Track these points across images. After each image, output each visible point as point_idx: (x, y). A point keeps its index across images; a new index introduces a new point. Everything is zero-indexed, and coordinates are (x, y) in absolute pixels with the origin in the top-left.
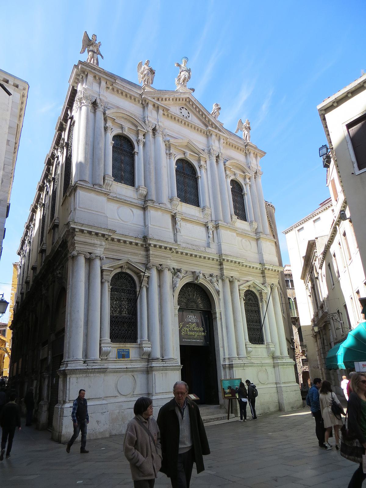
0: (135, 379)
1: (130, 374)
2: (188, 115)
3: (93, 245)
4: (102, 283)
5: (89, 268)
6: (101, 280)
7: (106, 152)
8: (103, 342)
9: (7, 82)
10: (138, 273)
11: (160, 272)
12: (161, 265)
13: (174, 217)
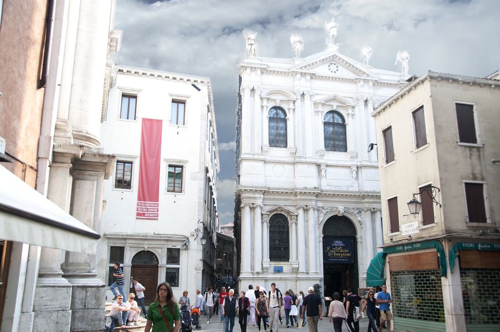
1: (284, 281)
4: (262, 223)
10: (288, 212)
11: (306, 210)
12: (307, 206)
13: (319, 166)
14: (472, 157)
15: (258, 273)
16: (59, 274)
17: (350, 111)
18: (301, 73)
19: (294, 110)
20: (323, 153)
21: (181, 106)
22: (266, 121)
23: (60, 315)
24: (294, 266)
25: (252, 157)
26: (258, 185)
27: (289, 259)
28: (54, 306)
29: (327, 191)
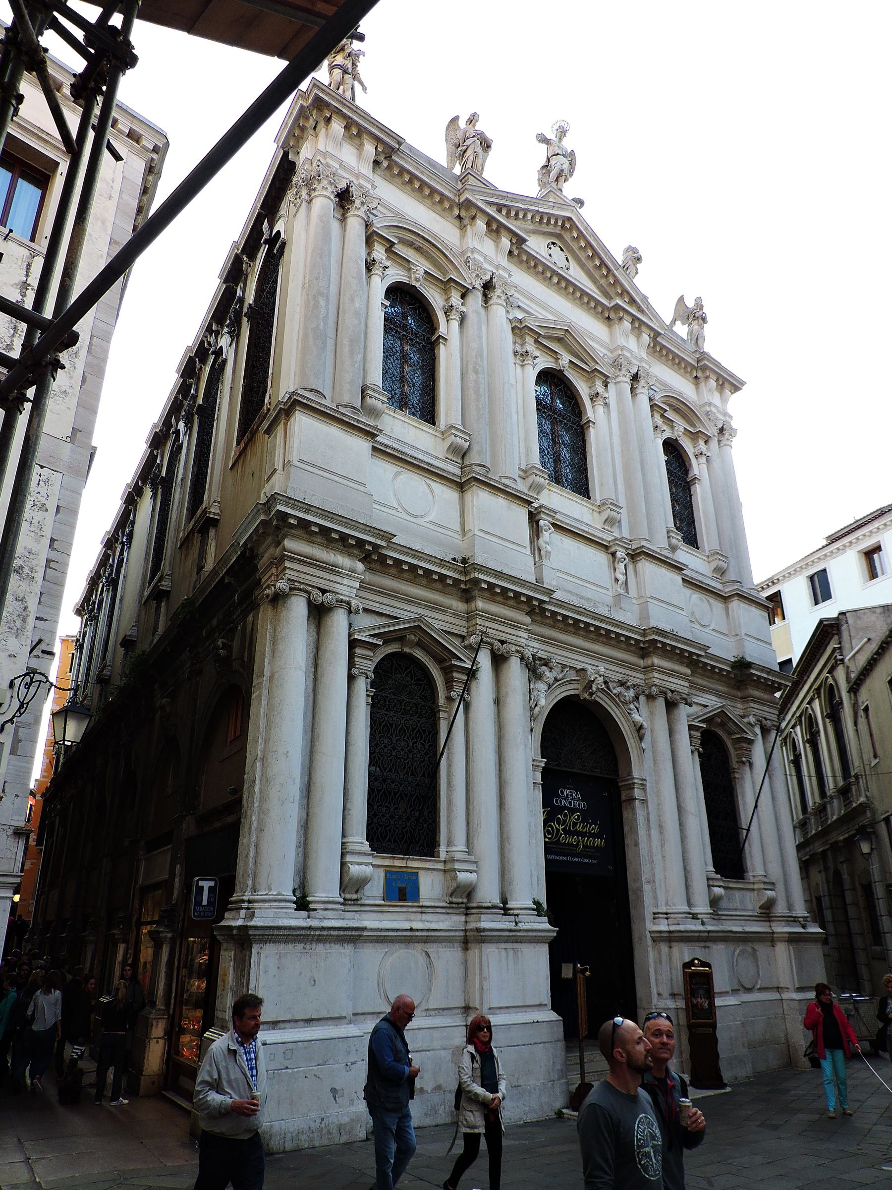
0: (431, 963)
1: (419, 946)
3: (332, 569)
4: (351, 678)
5: (318, 633)
6: (349, 670)
7: (370, 325)
10: (444, 658)
12: (502, 642)
13: (533, 518)
17: (599, 388)
19: (463, 319)
24: (462, 876)
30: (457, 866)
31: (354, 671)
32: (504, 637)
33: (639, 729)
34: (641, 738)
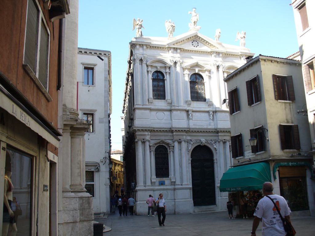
2: (198, 44)
4: (150, 152)
8: (152, 178)
9: (101, 54)
10: (168, 144)
11: (180, 143)
12: (180, 139)
14: (286, 109)
15: (148, 186)
16: (70, 191)
18: (174, 48)
19: (170, 73)
20: (190, 103)
21: (90, 71)
22: (151, 81)
23: (74, 212)
25: (142, 107)
26: (146, 126)
27: (169, 175)
28: (70, 208)
29: (193, 129)
30: (171, 179)
31: (151, 151)
32: (180, 138)
33: (215, 149)
34: (216, 151)
